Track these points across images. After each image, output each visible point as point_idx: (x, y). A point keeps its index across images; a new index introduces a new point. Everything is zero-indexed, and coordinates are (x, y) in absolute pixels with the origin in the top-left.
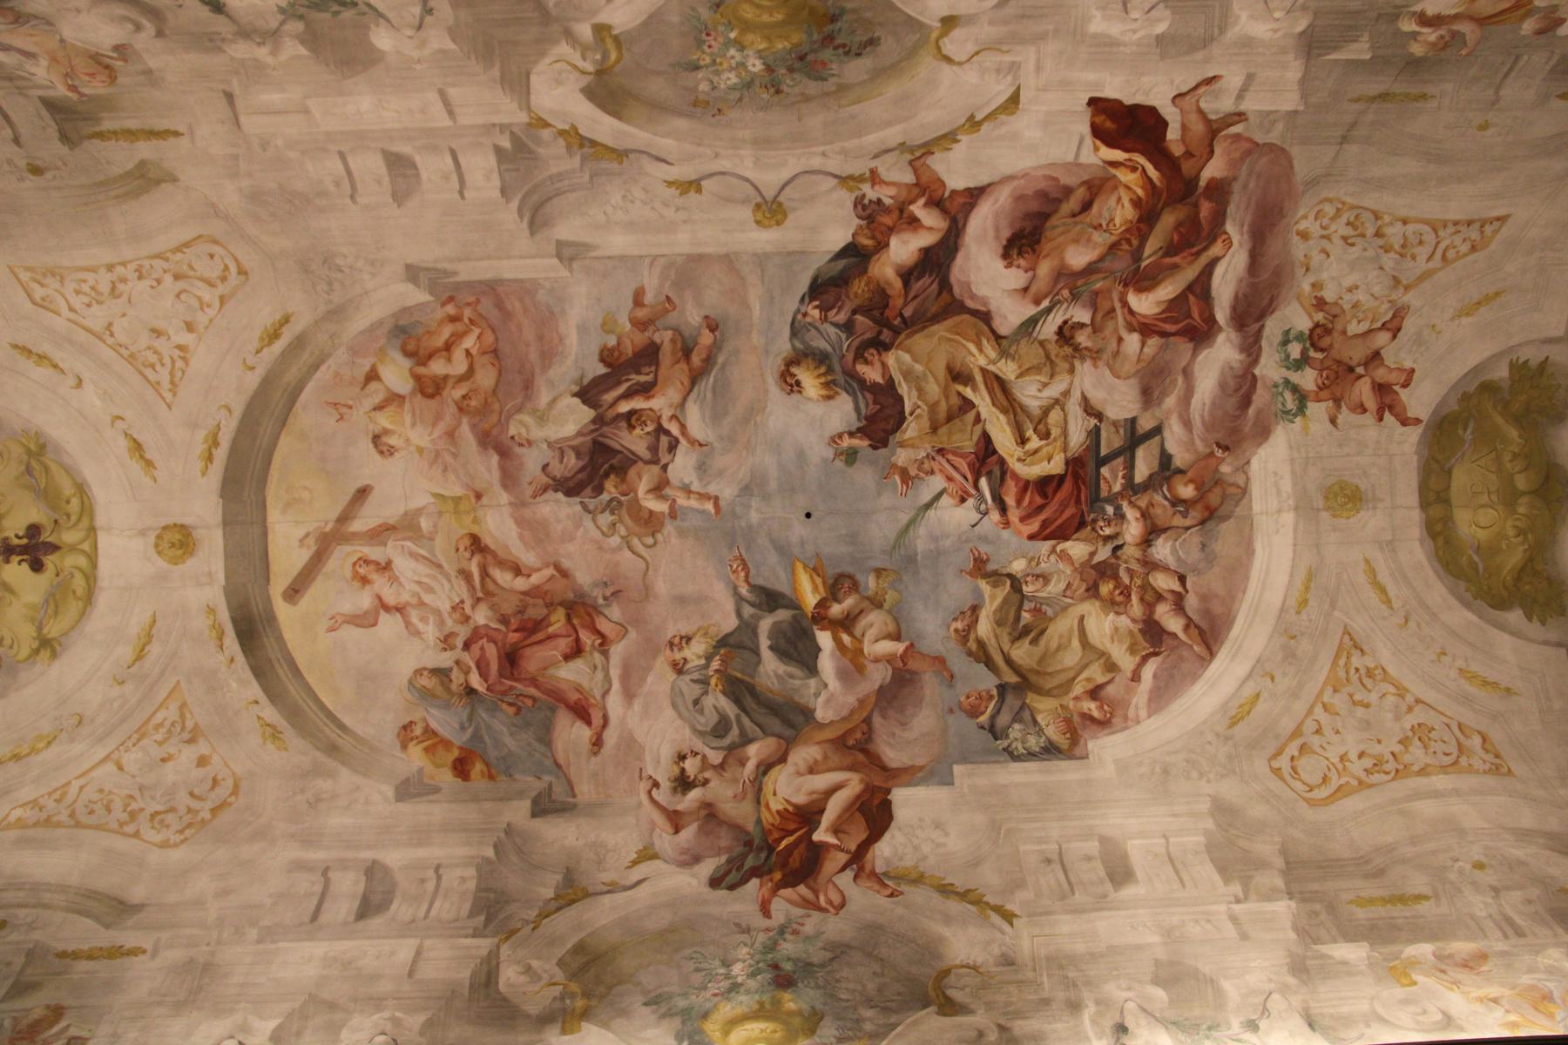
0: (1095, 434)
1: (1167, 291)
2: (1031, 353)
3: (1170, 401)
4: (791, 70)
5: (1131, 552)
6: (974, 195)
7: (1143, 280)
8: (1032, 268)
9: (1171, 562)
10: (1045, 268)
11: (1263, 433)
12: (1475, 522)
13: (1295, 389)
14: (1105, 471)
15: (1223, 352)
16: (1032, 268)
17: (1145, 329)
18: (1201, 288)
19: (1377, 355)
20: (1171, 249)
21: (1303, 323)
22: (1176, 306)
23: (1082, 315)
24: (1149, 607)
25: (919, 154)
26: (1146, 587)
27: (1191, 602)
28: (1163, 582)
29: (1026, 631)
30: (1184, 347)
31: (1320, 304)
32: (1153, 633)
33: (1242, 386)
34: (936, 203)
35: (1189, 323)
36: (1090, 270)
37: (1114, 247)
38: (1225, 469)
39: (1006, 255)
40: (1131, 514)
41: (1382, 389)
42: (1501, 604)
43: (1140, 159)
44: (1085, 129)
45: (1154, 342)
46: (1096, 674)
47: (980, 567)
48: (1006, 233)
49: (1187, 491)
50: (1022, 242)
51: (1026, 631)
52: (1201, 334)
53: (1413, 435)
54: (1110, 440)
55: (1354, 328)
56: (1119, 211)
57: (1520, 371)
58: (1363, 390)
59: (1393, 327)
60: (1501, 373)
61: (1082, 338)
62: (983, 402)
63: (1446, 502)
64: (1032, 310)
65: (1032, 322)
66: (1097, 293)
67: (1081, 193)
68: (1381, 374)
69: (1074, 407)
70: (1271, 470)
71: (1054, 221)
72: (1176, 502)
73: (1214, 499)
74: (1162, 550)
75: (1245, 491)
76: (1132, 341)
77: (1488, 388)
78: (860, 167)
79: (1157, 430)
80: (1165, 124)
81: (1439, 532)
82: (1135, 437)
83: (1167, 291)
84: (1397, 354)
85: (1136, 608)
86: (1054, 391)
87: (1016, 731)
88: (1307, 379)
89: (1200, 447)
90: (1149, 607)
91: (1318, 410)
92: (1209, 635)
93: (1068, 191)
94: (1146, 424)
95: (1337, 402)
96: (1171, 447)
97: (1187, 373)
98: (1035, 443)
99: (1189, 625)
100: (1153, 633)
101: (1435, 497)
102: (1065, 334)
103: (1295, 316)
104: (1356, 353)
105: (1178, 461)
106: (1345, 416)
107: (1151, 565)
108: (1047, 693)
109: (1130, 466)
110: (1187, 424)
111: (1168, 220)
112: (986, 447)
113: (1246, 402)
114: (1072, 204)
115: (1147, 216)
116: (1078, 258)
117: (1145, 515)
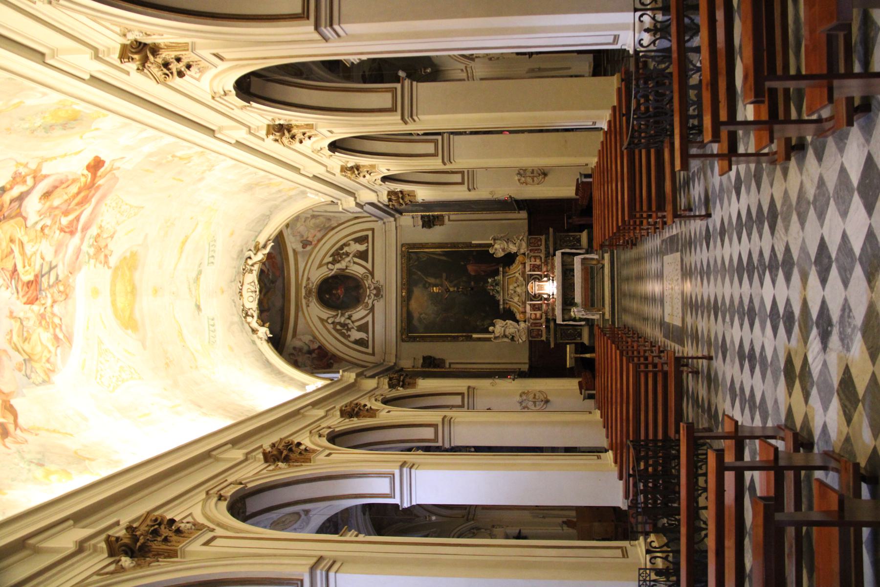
0: (42, 265)
1: (71, 217)
2: (32, 233)
3: (61, 256)
4: (44, 128)
5: (49, 309)
6: (46, 176)
7: (66, 213)
8: (44, 204)
9: (58, 314)
10: (48, 204)
11: (80, 269)
12: (121, 302)
13: (88, 254)
14: (43, 279)
15: (76, 240)
16: (44, 204)
17: (62, 230)
18: (78, 219)
19: (107, 245)
20: (78, 204)
21: (95, 233)
22: (71, 222)
23: (48, 222)
24: (54, 329)
25: (45, 160)
26: (53, 322)
27: (64, 327)
28: (57, 321)
29: (26, 339)
30: (68, 235)
31: (101, 227)
32: (56, 338)
33: (78, 251)
34: (34, 177)
35: (70, 230)
36: (57, 208)
37: (66, 201)
38: (71, 280)
39: (40, 199)
40: (49, 296)
41: (106, 256)
42: (127, 328)
43: (90, 175)
44: (86, 164)
45: (63, 234)
46: (46, 354)
47: (11, 315)
48: (45, 191)
49: (62, 288)
50: (47, 195)
51: (26, 339)
52: (72, 233)
53: (109, 272)
54: (46, 269)
55: (105, 236)
56: (74, 189)
57: (132, 252)
58: (102, 257)
59: (112, 237)
60: (128, 254)
61: (46, 231)
62: (16, 249)
63: (115, 294)
64: (38, 218)
65: (36, 223)
66: (55, 216)
67: (69, 182)
68: (107, 252)
69: (38, 256)
70: (81, 282)
71: (58, 189)
72: (60, 292)
73: (68, 291)
74: (56, 309)
75: (74, 288)
76: (58, 232)
77: (125, 258)
78: (24, 161)
79: (56, 266)
80: (103, 166)
81: (114, 303)
82: (51, 269)
83: (71, 217)
84: (110, 247)
85: (51, 330)
86: (34, 249)
87: (33, 375)
88: (92, 251)
89: (66, 273)
90: (54, 329)
91: (92, 261)
92: (69, 339)
93: (67, 180)
94: (54, 264)
95: (96, 259)
96: (59, 273)
97: (67, 246)
98: (27, 268)
99: (65, 336)
100: (56, 338)
101: (113, 293)
102: (42, 229)
103: (93, 231)
104: (103, 244)
105: (60, 278)
106: (98, 265)
107: (54, 314)
108: (36, 362)
109: (49, 278)
110: (64, 264)
111: (82, 194)
112: (15, 270)
113: (77, 258)
114: (64, 186)
115: (78, 194)
116: (56, 203)
117: (52, 296)
